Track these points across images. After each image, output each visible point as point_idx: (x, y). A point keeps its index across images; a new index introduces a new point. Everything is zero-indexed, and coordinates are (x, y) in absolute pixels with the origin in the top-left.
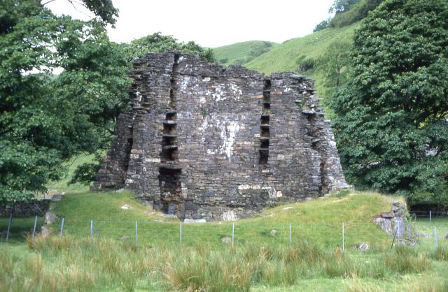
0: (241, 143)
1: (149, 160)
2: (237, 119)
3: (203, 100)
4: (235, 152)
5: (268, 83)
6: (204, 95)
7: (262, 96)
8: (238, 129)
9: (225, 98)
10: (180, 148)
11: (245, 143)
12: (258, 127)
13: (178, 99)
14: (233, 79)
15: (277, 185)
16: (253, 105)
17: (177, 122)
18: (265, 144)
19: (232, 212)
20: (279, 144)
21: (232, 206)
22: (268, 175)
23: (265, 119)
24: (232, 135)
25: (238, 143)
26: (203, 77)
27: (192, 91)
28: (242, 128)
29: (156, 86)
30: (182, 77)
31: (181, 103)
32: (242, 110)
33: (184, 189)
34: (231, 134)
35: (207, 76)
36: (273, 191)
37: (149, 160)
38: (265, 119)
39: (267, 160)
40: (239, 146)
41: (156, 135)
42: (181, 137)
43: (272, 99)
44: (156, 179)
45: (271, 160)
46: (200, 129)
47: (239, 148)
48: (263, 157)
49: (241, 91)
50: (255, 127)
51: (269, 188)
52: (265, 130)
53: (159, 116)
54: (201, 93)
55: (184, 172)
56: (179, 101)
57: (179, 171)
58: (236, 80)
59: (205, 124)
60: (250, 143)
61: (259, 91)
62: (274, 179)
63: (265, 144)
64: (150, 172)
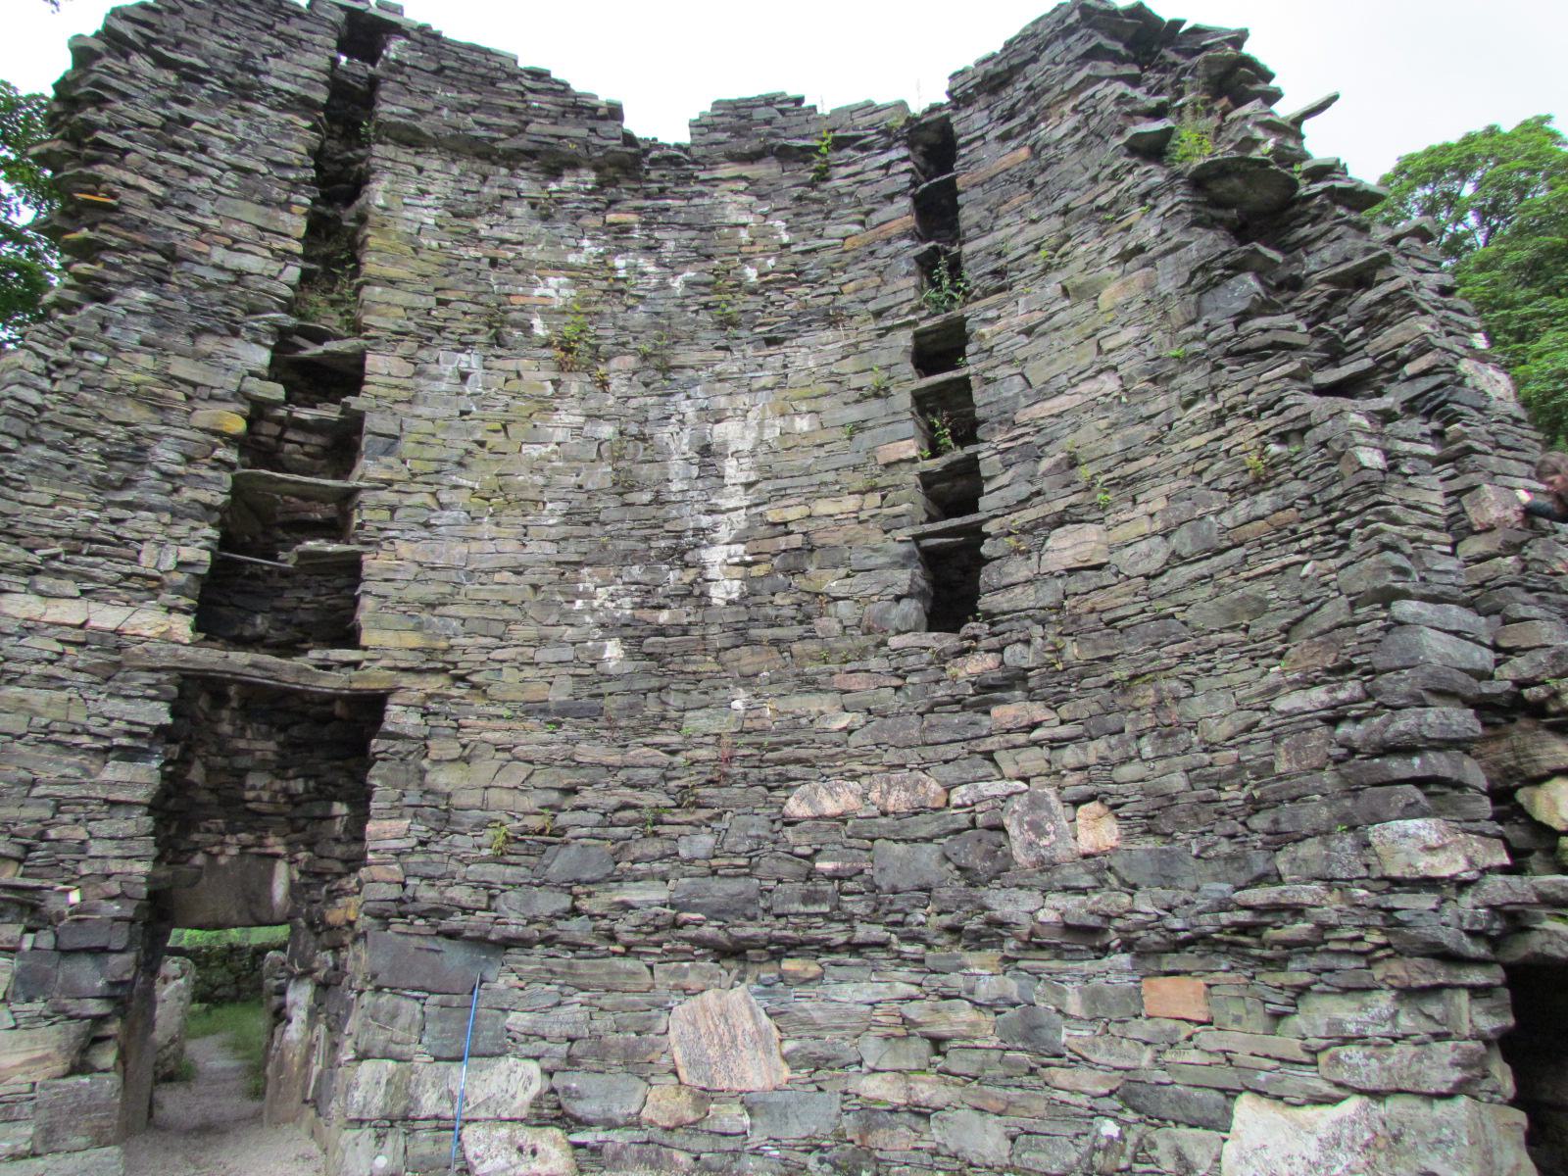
0: (792, 514)
1: (71, 612)
2: (767, 378)
3: (555, 289)
4: (755, 571)
5: (932, 142)
6: (559, 268)
7: (910, 221)
8: (771, 434)
9: (689, 274)
10: (372, 564)
11: (822, 507)
12: (903, 400)
13: (371, 265)
14: (728, 170)
15: (1070, 756)
16: (853, 282)
17: (356, 403)
18: (954, 491)
19: (739, 994)
20: (1045, 464)
21: (732, 952)
22: (988, 692)
23: (938, 350)
24: (734, 471)
25: (773, 516)
26: (555, 174)
27: (475, 238)
28: (802, 424)
29: (180, 149)
30: (404, 155)
31: (399, 297)
32: (802, 321)
33: (386, 831)
34: (730, 467)
35: (574, 165)
36: (1036, 803)
37: (71, 612)
38: (938, 350)
39: (975, 594)
40: (783, 527)
41: (165, 454)
42: (388, 496)
43: (969, 216)
44: (129, 755)
45: (1011, 584)
46: (533, 451)
47: (782, 543)
48: (951, 586)
49: (780, 224)
50: (874, 406)
51: (998, 788)
52: (949, 413)
53: (208, 344)
54: (533, 253)
55: (399, 716)
56: (392, 282)
57: (373, 704)
58: (747, 170)
59: (568, 416)
60: (851, 503)
61: (890, 198)
62: (1038, 711)
63: (954, 491)
64: (39, 697)
